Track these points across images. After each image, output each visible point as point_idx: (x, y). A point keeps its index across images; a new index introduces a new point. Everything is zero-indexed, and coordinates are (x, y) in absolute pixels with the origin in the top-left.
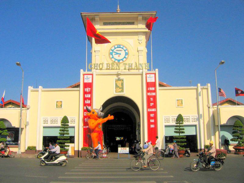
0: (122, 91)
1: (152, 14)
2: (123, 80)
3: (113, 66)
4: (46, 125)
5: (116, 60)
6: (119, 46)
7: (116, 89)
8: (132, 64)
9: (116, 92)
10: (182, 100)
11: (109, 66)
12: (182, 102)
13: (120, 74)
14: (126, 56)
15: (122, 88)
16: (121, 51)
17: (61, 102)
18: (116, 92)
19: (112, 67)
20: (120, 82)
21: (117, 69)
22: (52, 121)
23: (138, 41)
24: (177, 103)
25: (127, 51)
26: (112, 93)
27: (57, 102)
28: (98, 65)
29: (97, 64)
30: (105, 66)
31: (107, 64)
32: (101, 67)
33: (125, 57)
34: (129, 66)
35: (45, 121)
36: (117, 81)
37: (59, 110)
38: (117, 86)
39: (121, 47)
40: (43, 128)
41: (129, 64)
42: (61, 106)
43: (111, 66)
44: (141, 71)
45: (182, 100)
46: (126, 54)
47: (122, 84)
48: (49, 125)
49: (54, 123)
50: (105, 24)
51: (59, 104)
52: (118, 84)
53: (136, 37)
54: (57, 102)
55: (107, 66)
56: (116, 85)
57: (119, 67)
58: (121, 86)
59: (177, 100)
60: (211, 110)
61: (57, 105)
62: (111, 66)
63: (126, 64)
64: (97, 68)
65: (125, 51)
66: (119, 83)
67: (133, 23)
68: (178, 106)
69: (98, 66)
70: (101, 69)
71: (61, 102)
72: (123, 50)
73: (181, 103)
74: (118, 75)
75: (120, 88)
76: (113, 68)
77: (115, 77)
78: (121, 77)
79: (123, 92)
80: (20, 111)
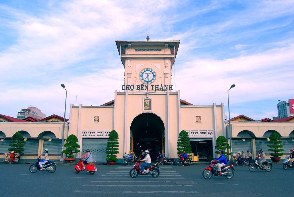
0: (150, 109)
1: (177, 42)
2: (150, 100)
3: (143, 87)
4: (85, 137)
6: (148, 70)
7: (144, 107)
8: (158, 86)
9: (144, 109)
10: (200, 116)
11: (139, 87)
12: (200, 118)
13: (148, 94)
14: (154, 78)
15: (150, 106)
16: (149, 73)
17: (98, 117)
18: (144, 109)
19: (141, 88)
20: (148, 101)
21: (145, 90)
22: (90, 134)
23: (164, 66)
24: (196, 119)
25: (154, 74)
26: (141, 110)
27: (95, 117)
28: (130, 86)
29: (129, 86)
33: (153, 79)
34: (156, 88)
35: (84, 134)
36: (145, 100)
37: (96, 124)
38: (145, 105)
39: (150, 70)
40: (82, 139)
42: (98, 120)
43: (140, 87)
44: (166, 91)
45: (200, 116)
46: (154, 76)
47: (150, 103)
48: (88, 136)
49: (92, 135)
51: (96, 119)
52: (146, 103)
53: (162, 61)
54: (95, 117)
55: (137, 87)
57: (147, 88)
58: (148, 104)
59: (196, 117)
60: (225, 125)
62: (140, 87)
63: (154, 86)
64: (129, 88)
67: (160, 50)
68: (197, 122)
69: (130, 88)
70: (132, 90)
71: (98, 117)
72: (151, 73)
74: (146, 94)
75: (148, 106)
76: (142, 89)
77: (145, 97)
78: (149, 97)
79: (151, 110)
80: (63, 124)
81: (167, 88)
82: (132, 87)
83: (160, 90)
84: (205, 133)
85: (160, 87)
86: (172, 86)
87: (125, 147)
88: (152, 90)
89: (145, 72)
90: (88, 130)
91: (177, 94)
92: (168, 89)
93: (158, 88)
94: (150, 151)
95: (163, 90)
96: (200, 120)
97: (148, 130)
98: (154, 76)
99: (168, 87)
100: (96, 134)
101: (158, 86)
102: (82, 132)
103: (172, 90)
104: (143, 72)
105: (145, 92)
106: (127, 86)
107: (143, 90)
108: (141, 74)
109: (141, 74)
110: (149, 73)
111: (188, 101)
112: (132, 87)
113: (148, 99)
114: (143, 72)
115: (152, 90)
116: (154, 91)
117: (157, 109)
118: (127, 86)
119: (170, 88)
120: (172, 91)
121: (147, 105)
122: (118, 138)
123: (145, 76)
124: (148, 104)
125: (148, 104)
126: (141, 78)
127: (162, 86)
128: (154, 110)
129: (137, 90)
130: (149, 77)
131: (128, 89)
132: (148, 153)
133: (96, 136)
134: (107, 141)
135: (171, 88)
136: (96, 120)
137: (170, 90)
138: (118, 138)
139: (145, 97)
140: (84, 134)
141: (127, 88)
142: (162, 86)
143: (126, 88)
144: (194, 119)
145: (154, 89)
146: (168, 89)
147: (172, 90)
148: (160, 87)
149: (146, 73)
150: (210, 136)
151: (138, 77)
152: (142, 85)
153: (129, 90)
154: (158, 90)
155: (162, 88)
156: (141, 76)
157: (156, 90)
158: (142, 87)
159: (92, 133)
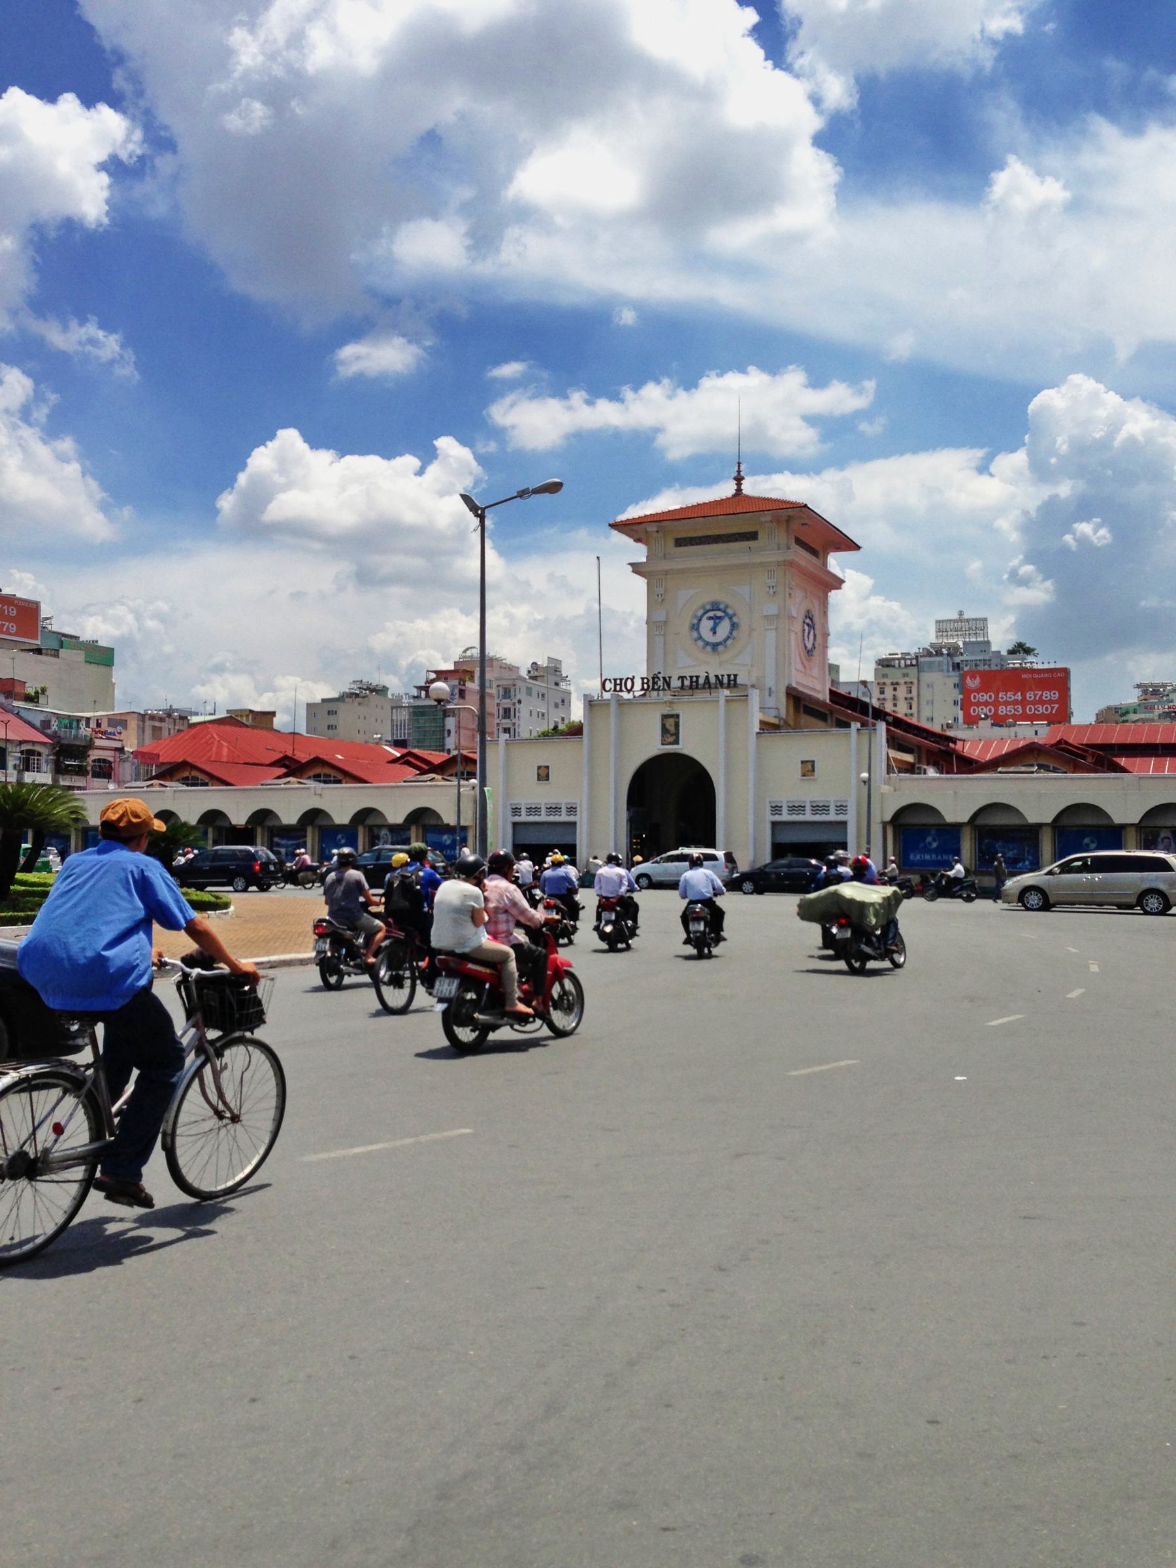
0: (676, 742)
2: (678, 716)
5: (707, 644)
6: (715, 606)
8: (697, 677)
12: (813, 766)
14: (735, 633)
15: (677, 734)
17: (547, 767)
20: (672, 721)
27: (539, 768)
31: (643, 679)
37: (543, 787)
38: (665, 730)
39: (722, 607)
41: (691, 677)
42: (547, 778)
46: (734, 626)
47: (677, 725)
50: (679, 542)
51: (543, 772)
52: (668, 726)
54: (539, 768)
56: (663, 726)
58: (672, 729)
59: (803, 762)
61: (538, 775)
66: (670, 724)
67: (753, 536)
68: (804, 775)
70: (629, 691)
71: (547, 767)
73: (810, 767)
75: (672, 735)
82: (629, 682)
83: (704, 688)
84: (825, 809)
85: (701, 681)
86: (735, 676)
89: (711, 614)
96: (813, 770)
101: (697, 677)
106: (615, 680)
107: (658, 690)
110: (719, 618)
112: (629, 682)
114: (699, 614)
118: (615, 680)
124: (670, 728)
125: (670, 728)
126: (695, 635)
127: (707, 677)
128: (685, 747)
130: (718, 630)
131: (618, 688)
136: (543, 774)
141: (616, 685)
142: (707, 677)
145: (687, 683)
148: (701, 681)
149: (710, 618)
152: (655, 677)
156: (695, 627)
158: (654, 683)
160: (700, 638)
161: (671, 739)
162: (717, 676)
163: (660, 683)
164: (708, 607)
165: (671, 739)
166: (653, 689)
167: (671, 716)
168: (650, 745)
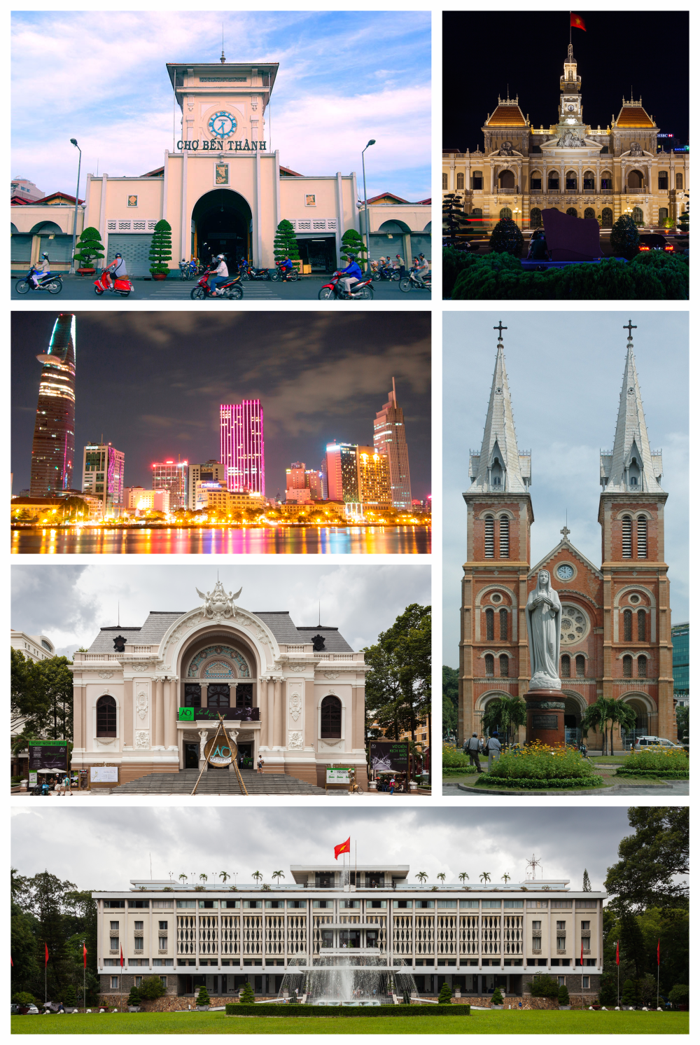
0: (226, 182)
2: (227, 166)
4: (112, 231)
6: (223, 114)
8: (241, 142)
12: (314, 199)
14: (234, 129)
15: (227, 177)
17: (136, 197)
20: (223, 169)
22: (123, 225)
25: (234, 122)
27: (130, 197)
29: (190, 142)
30: (201, 145)
32: (195, 147)
34: (237, 145)
35: (112, 226)
36: (218, 166)
37: (132, 209)
38: (218, 174)
39: (227, 114)
42: (136, 202)
43: (210, 144)
44: (254, 152)
46: (234, 125)
47: (226, 172)
48: (118, 230)
51: (133, 200)
52: (220, 172)
54: (130, 197)
56: (217, 172)
57: (222, 146)
58: (224, 174)
62: (210, 144)
65: (232, 121)
70: (195, 149)
71: (136, 197)
74: (220, 157)
77: (217, 161)
78: (225, 161)
81: (256, 147)
83: (244, 149)
84: (322, 225)
85: (243, 144)
86: (265, 142)
87: (182, 248)
88: (231, 149)
90: (118, 219)
91: (273, 156)
92: (258, 147)
93: (240, 145)
94: (226, 256)
95: (249, 149)
97: (222, 219)
98: (234, 125)
99: (258, 145)
100: (132, 225)
101: (241, 142)
102: (107, 225)
103: (265, 149)
104: (214, 117)
105: (217, 152)
108: (211, 121)
109: (211, 121)
111: (292, 168)
113: (223, 166)
114: (214, 117)
115: (231, 149)
116: (233, 152)
117: (238, 183)
118: (186, 142)
119: (261, 145)
120: (265, 152)
121: (221, 176)
122: (170, 234)
123: (217, 124)
125: (222, 174)
126: (211, 129)
128: (234, 185)
129: (204, 149)
130: (225, 126)
132: (223, 260)
133: (132, 231)
134: (151, 239)
135: (263, 145)
136: (133, 202)
137: (261, 149)
138: (170, 234)
139: (217, 161)
140: (112, 226)
141: (186, 145)
143: (184, 145)
144: (304, 201)
145: (234, 147)
146: (258, 147)
147: (265, 149)
148: (243, 144)
150: (332, 230)
151: (205, 126)
152: (213, 141)
153: (190, 149)
154: (240, 149)
155: (248, 146)
156: (211, 125)
157: (236, 149)
159: (125, 225)
160: (214, 131)
161: (223, 180)
162: (253, 142)
163: (216, 145)
164: (219, 114)
165: (223, 180)
166: (211, 149)
167: (223, 166)
168: (210, 185)
